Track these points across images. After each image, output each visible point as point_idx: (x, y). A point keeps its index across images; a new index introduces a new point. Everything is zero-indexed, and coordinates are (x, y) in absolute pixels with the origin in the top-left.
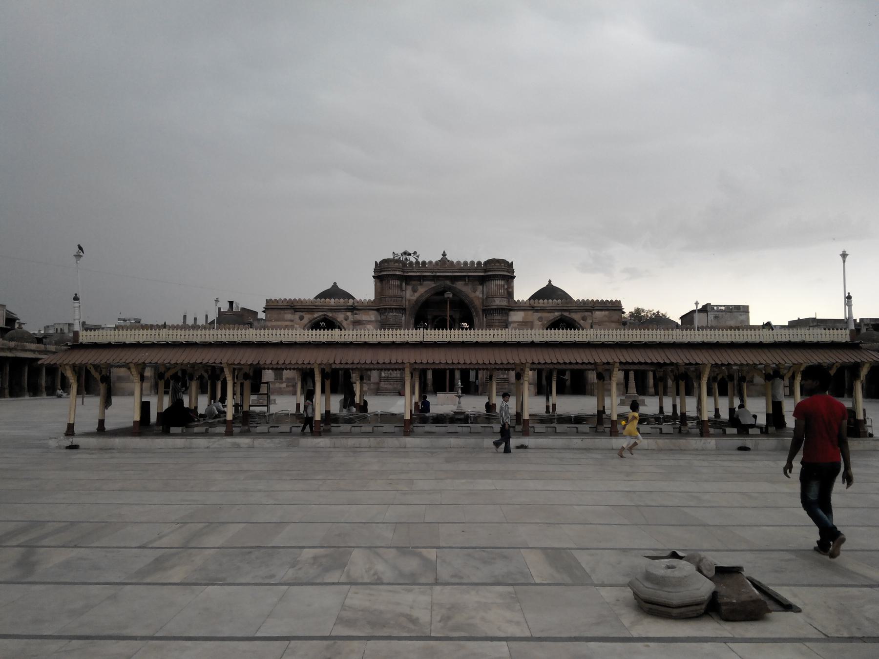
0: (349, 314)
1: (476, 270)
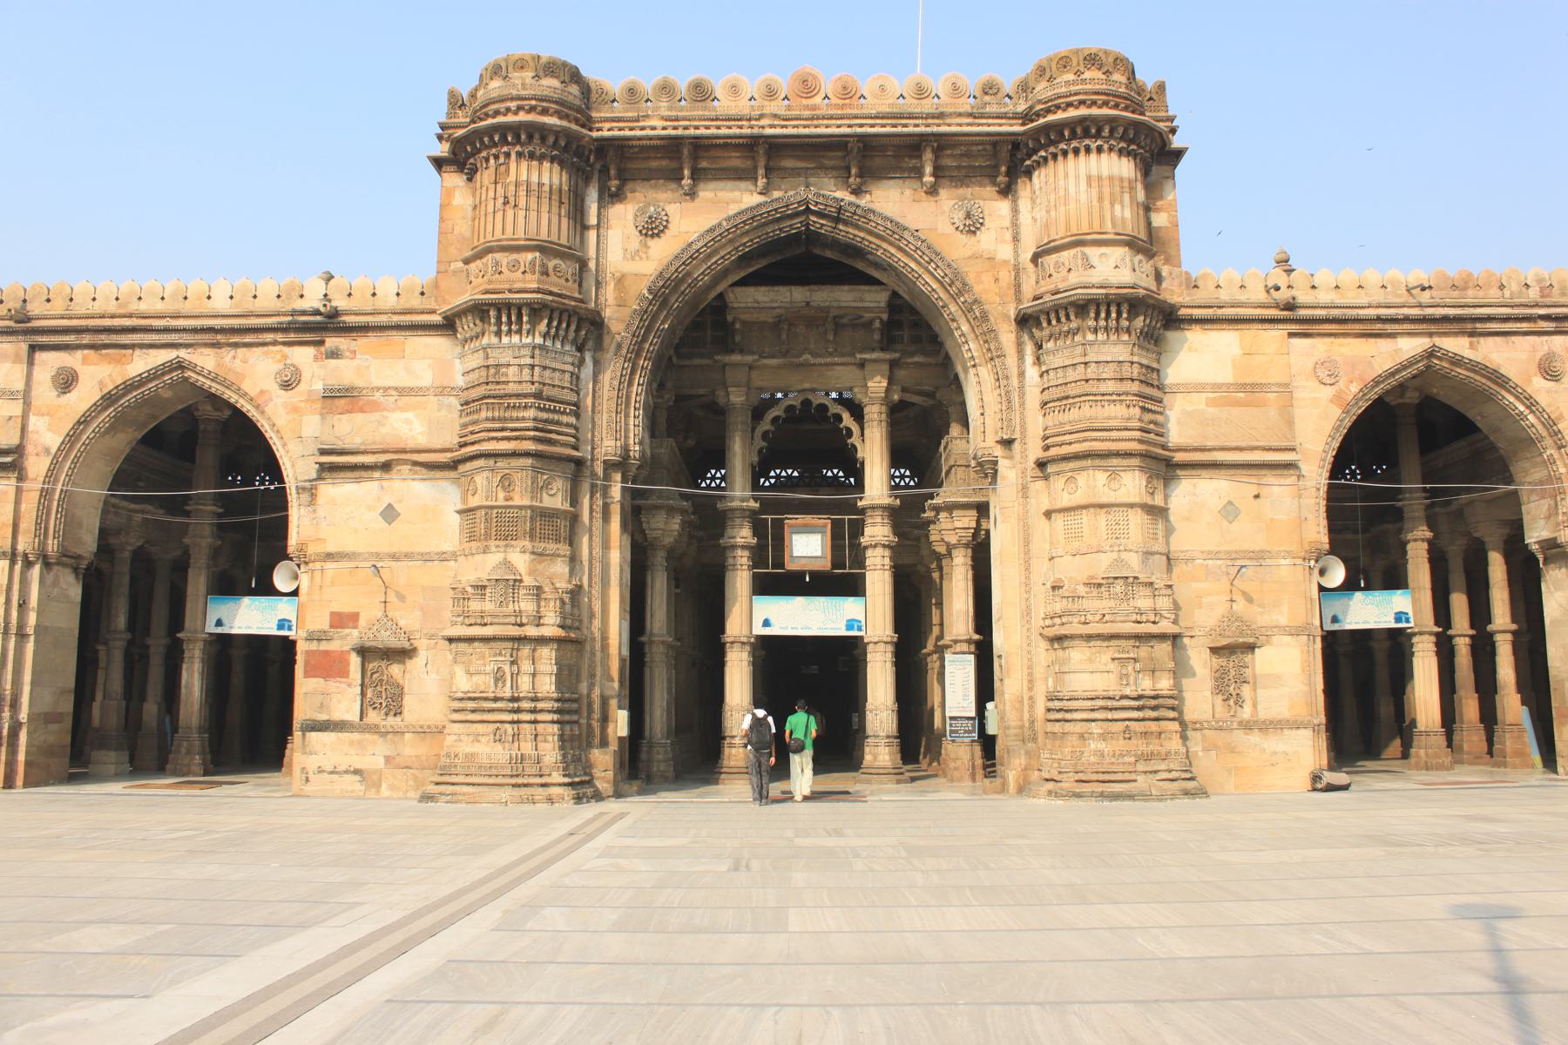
0: (303, 356)
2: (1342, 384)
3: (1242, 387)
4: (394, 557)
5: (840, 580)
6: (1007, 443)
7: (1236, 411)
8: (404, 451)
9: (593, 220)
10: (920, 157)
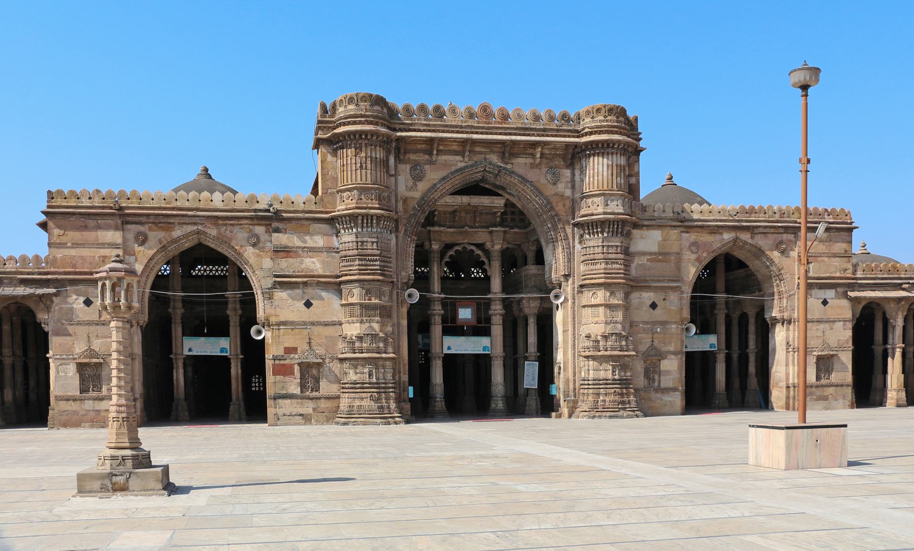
0: (260, 230)
1: (558, 132)
2: (700, 253)
3: (660, 254)
4: (313, 324)
5: (480, 329)
6: (566, 277)
7: (658, 264)
8: (313, 276)
10: (534, 149)
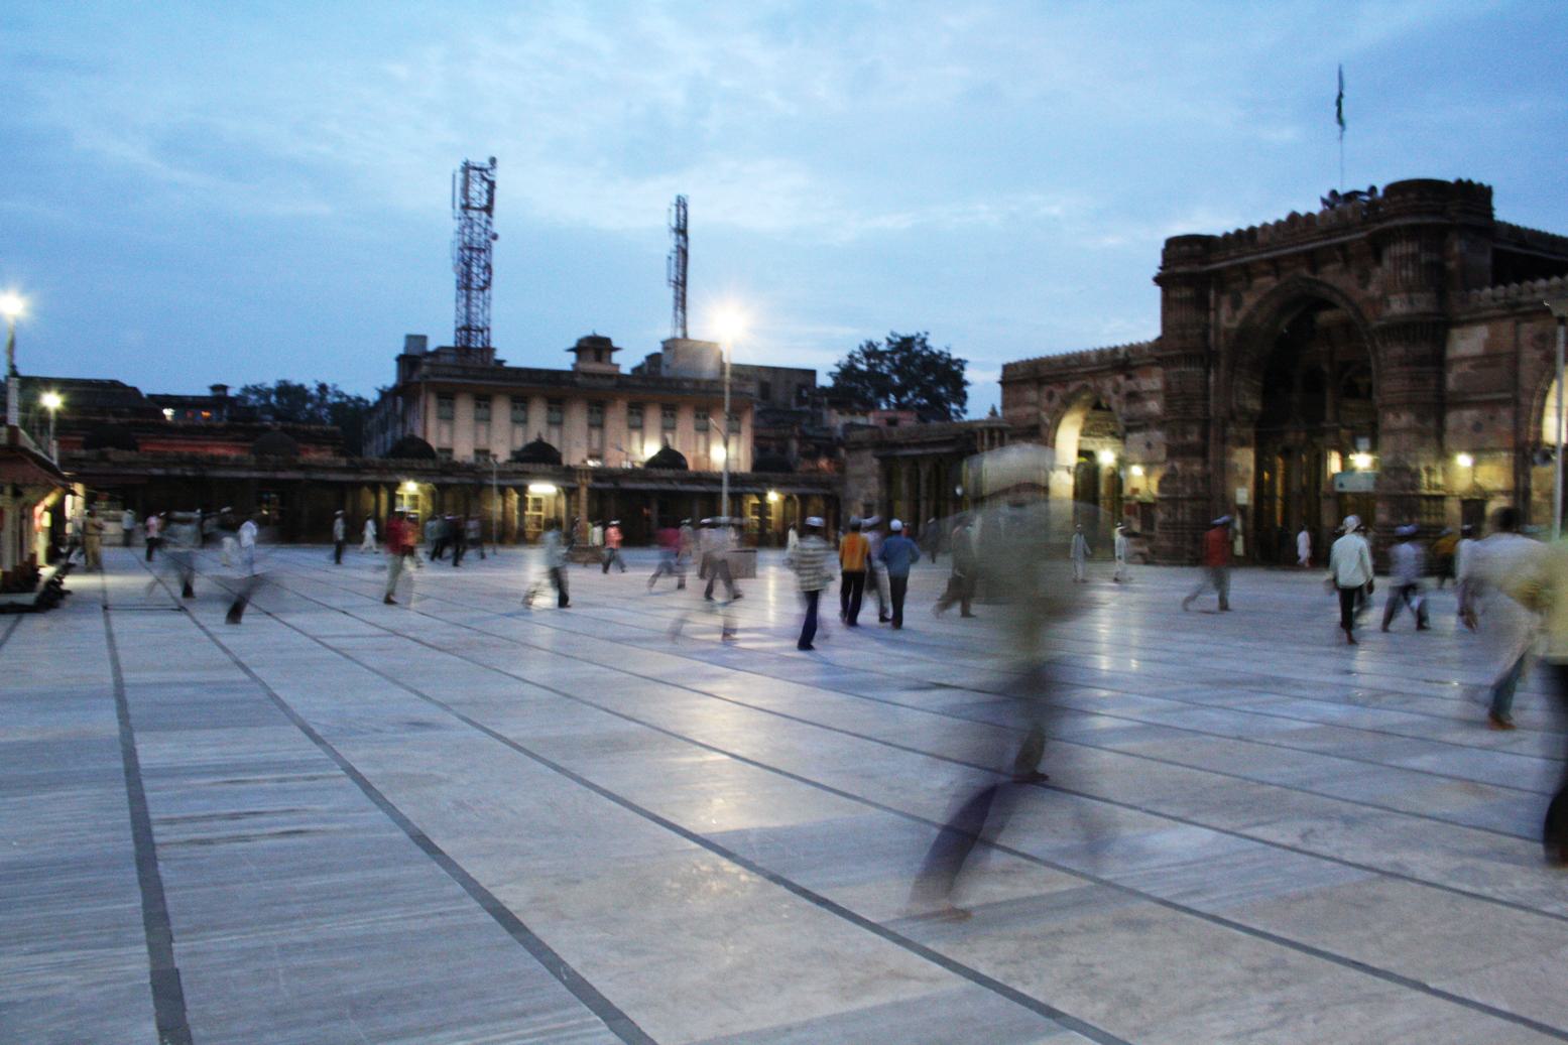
0: (1121, 379)
9: (1212, 305)
